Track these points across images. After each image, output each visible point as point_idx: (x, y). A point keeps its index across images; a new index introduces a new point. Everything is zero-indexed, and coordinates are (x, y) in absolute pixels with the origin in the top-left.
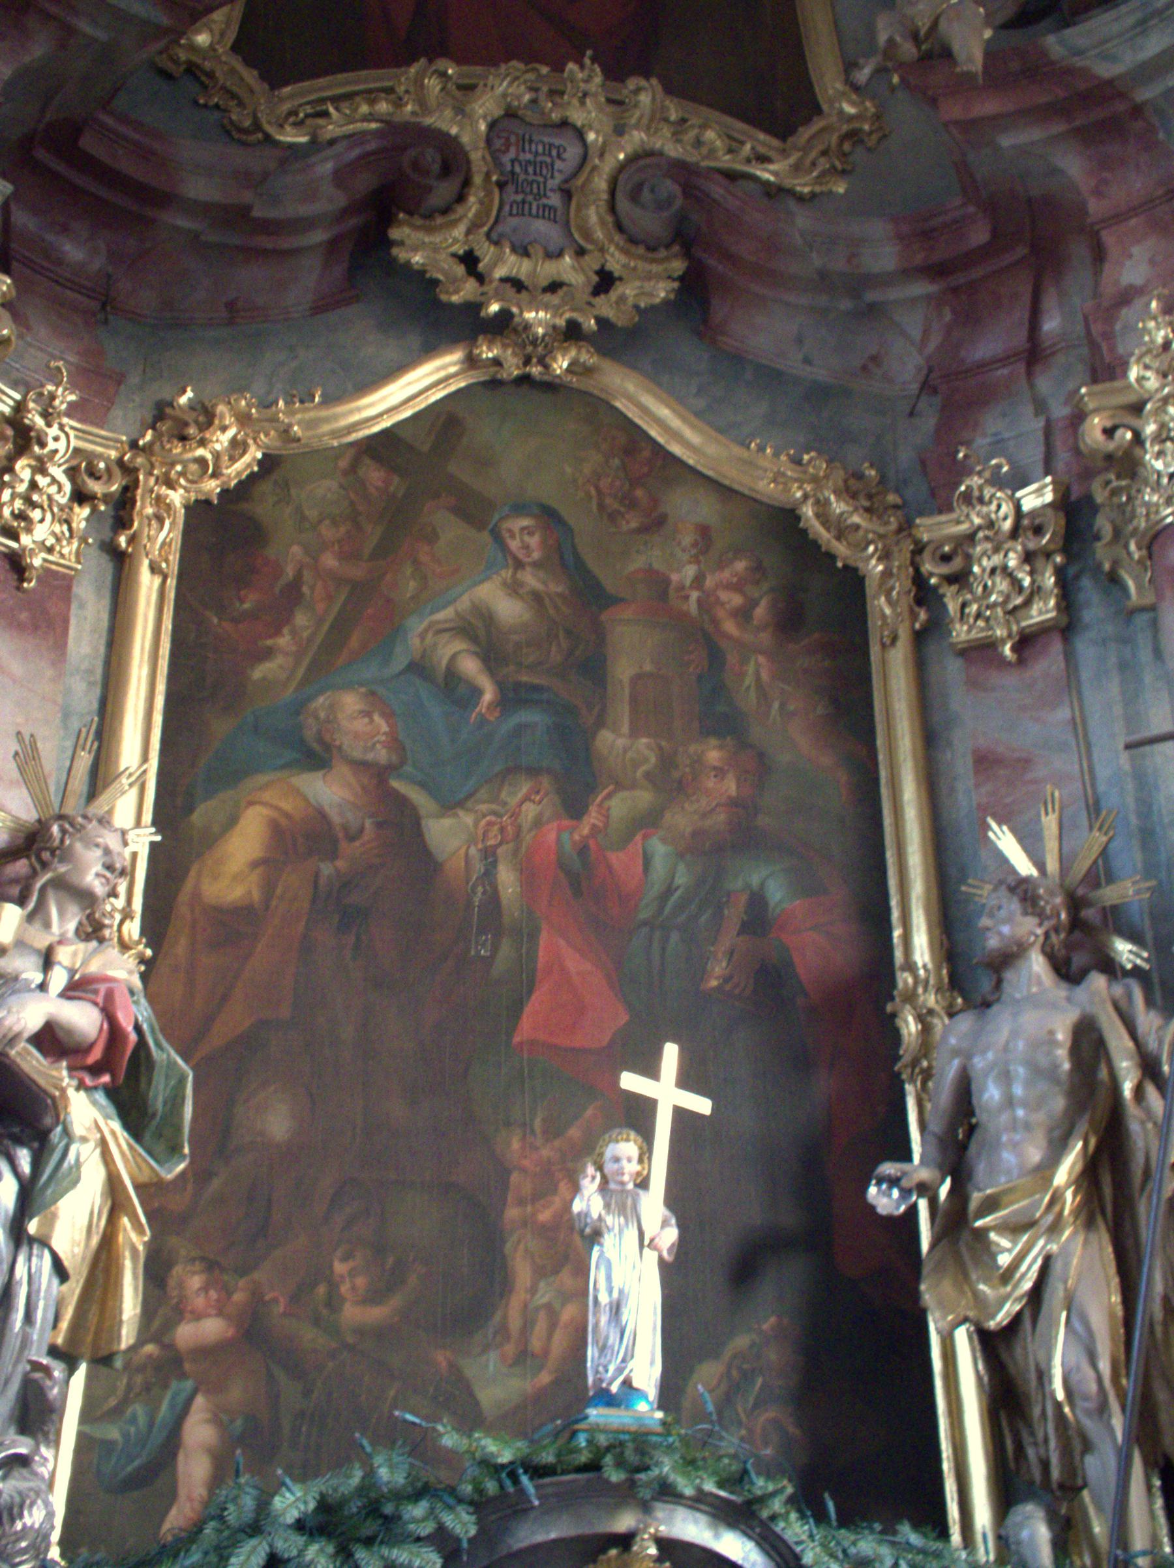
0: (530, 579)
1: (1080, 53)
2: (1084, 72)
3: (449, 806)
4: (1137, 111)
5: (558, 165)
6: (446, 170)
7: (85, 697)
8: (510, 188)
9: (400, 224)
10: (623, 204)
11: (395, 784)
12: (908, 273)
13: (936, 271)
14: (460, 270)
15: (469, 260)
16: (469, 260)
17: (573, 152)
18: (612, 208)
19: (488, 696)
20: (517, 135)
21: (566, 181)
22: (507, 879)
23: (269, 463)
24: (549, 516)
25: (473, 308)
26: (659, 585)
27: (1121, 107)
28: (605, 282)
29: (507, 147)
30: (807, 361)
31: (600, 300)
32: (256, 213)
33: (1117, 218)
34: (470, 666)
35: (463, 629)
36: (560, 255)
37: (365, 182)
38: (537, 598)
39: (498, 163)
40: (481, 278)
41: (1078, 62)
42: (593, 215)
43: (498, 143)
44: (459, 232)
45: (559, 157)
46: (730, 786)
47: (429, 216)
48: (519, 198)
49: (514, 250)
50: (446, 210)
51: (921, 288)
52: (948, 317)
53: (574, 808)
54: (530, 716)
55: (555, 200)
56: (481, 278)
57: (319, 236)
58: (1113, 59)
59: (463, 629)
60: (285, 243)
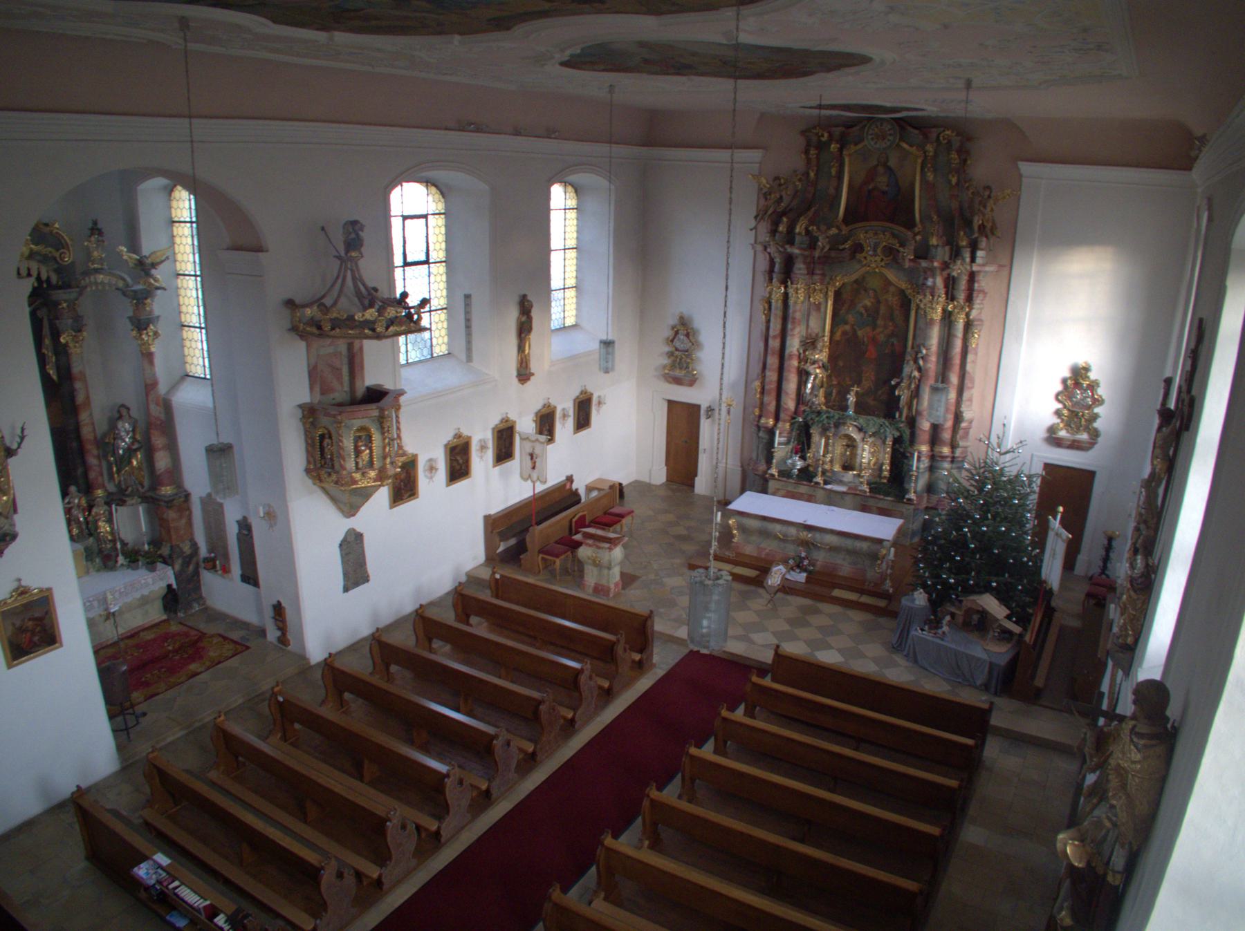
0: (872, 300)
3: (860, 329)
7: (822, 315)
11: (855, 327)
15: (865, 258)
16: (865, 258)
19: (865, 315)
22: (865, 339)
23: (843, 284)
24: (875, 291)
26: (886, 300)
28: (882, 260)
34: (864, 312)
35: (863, 307)
38: (872, 303)
46: (891, 328)
53: (874, 329)
54: (870, 319)
59: (863, 307)
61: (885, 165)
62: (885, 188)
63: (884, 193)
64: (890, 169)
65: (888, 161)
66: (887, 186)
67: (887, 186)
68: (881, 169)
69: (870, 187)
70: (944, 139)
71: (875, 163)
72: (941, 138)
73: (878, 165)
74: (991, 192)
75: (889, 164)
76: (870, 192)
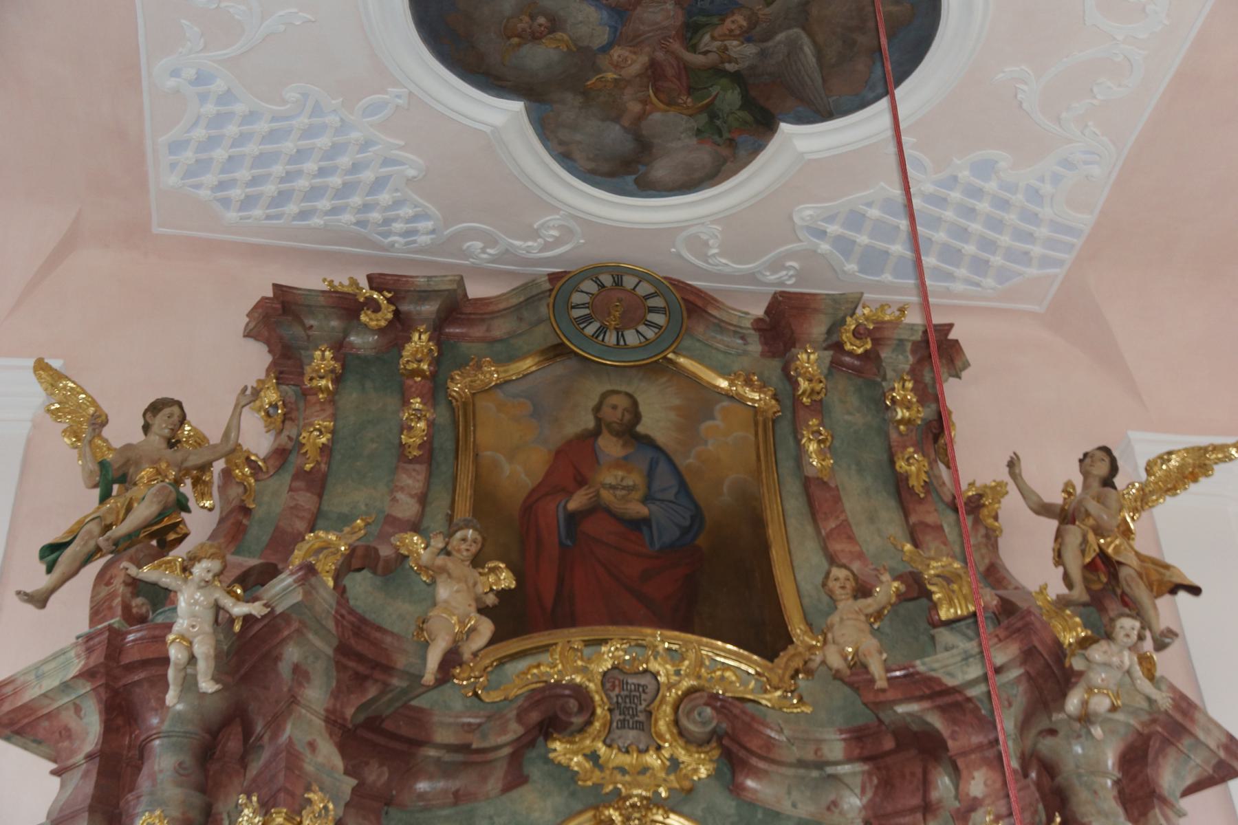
1: (934, 670)
2: (937, 681)
4: (969, 700)
5: (643, 696)
6: (581, 709)
8: (617, 712)
9: (555, 739)
10: (684, 722)
12: (849, 760)
13: (865, 759)
14: (588, 765)
17: (651, 688)
18: (676, 722)
20: (619, 680)
21: (648, 705)
25: (598, 786)
27: (959, 698)
29: (614, 687)
30: (794, 805)
31: (672, 777)
32: (474, 746)
33: (964, 754)
36: (647, 751)
37: (535, 717)
39: (609, 698)
40: (601, 768)
41: (933, 674)
42: (662, 726)
43: (608, 685)
44: (588, 742)
45: (644, 691)
47: (572, 734)
48: (622, 717)
49: (620, 749)
50: (582, 730)
51: (859, 767)
52: (875, 781)
55: (642, 717)
56: (601, 768)
57: (506, 751)
58: (951, 675)
60: (491, 756)
61: (629, 432)
62: (637, 509)
63: (638, 525)
64: (647, 442)
65: (637, 417)
66: (647, 499)
67: (647, 499)
68: (610, 447)
69: (573, 505)
70: (856, 334)
71: (590, 423)
72: (846, 337)
73: (596, 433)
74: (1114, 469)
75: (640, 429)
76: (573, 519)
